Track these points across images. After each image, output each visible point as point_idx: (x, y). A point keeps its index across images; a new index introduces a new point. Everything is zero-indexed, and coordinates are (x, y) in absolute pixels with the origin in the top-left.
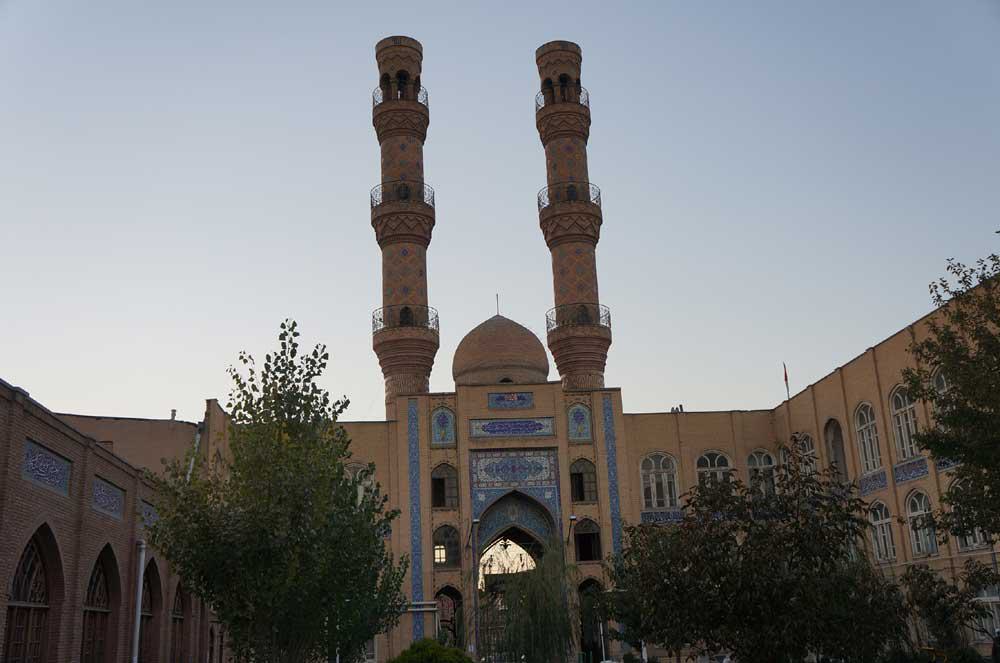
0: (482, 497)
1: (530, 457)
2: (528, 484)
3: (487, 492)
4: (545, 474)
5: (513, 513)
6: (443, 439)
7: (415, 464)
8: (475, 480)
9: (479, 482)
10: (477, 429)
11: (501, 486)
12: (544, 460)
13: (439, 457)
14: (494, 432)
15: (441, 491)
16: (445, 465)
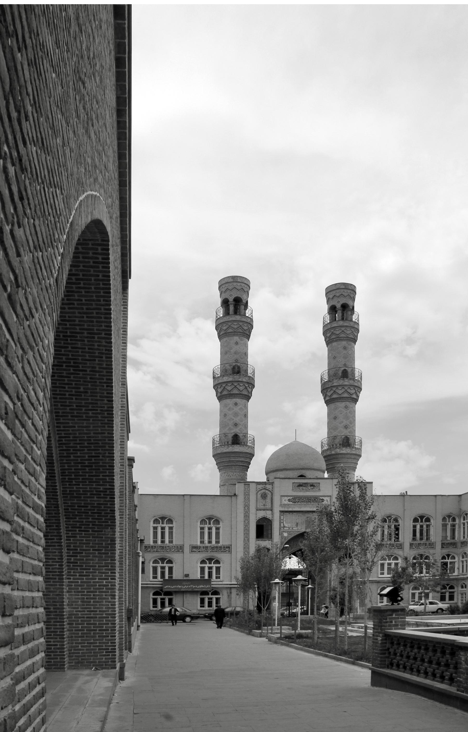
0: (285, 535)
3: (289, 532)
6: (264, 505)
7: (247, 516)
8: (282, 525)
9: (284, 527)
10: (285, 501)
13: (261, 514)
14: (295, 502)
15: (263, 529)
16: (264, 519)
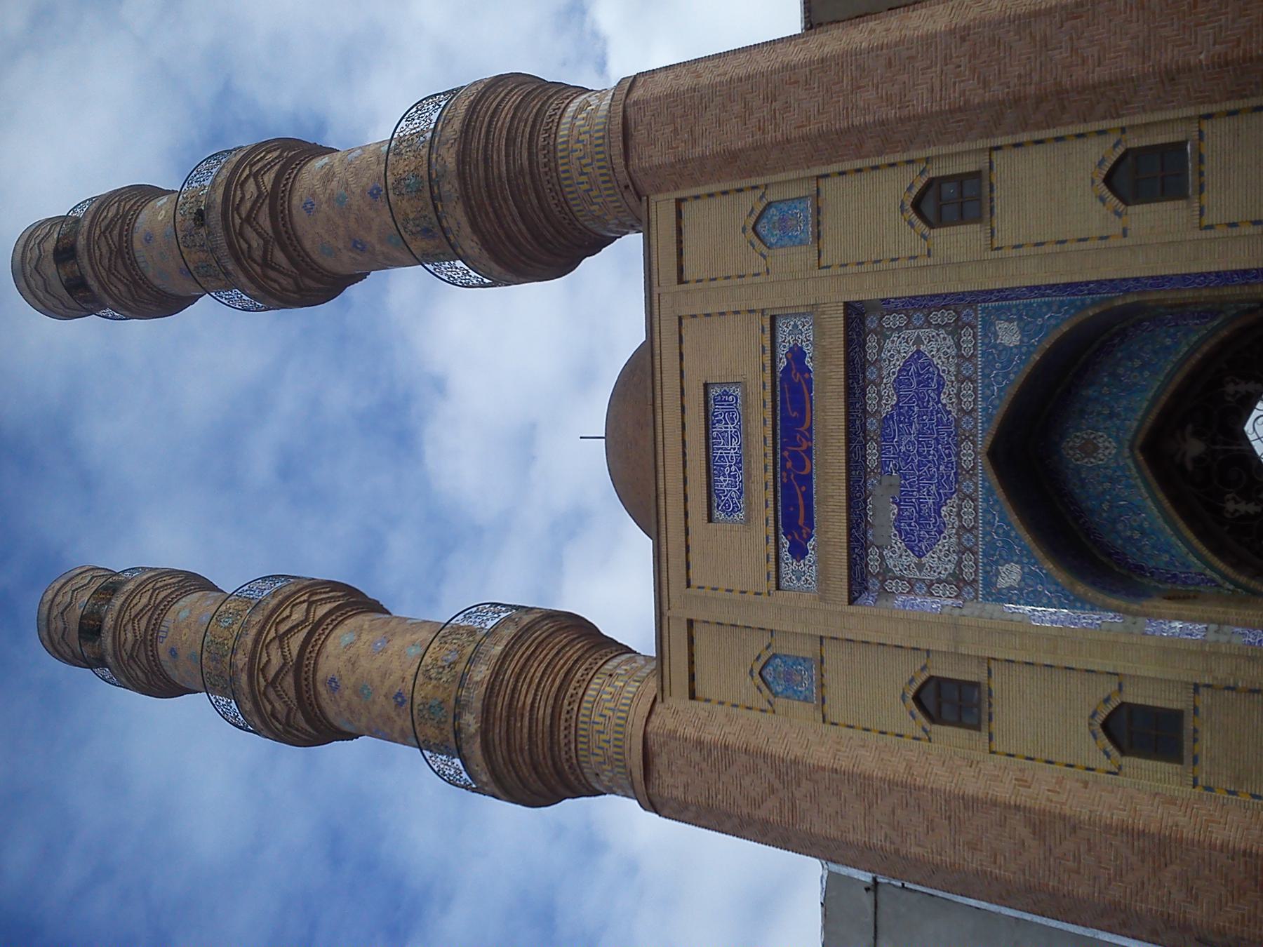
0: (1010, 575)
1: (882, 398)
2: (975, 405)
4: (938, 348)
5: (1090, 449)
11: (976, 501)
12: (893, 351)
